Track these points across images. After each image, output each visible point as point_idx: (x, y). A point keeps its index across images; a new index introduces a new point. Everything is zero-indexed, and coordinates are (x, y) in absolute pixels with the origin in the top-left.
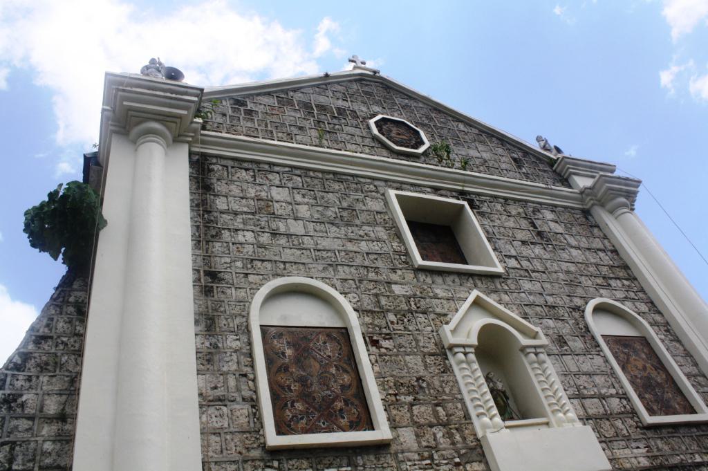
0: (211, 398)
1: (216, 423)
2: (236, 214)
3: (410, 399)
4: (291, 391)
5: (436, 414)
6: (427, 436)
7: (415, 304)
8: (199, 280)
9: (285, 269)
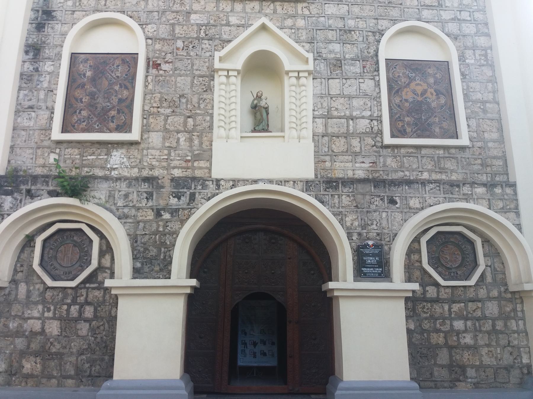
0: (26, 107)
1: (26, 123)
3: (169, 111)
4: (82, 102)
5: (185, 124)
6: (171, 139)
7: (205, 32)
8: (37, 19)
9: (105, 5)
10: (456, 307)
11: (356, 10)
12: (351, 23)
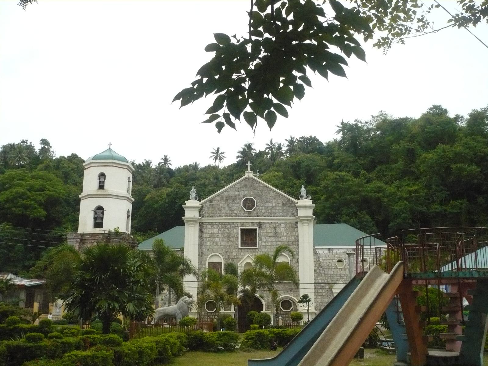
2: (207, 238)
10: (286, 315)
11: (269, 250)
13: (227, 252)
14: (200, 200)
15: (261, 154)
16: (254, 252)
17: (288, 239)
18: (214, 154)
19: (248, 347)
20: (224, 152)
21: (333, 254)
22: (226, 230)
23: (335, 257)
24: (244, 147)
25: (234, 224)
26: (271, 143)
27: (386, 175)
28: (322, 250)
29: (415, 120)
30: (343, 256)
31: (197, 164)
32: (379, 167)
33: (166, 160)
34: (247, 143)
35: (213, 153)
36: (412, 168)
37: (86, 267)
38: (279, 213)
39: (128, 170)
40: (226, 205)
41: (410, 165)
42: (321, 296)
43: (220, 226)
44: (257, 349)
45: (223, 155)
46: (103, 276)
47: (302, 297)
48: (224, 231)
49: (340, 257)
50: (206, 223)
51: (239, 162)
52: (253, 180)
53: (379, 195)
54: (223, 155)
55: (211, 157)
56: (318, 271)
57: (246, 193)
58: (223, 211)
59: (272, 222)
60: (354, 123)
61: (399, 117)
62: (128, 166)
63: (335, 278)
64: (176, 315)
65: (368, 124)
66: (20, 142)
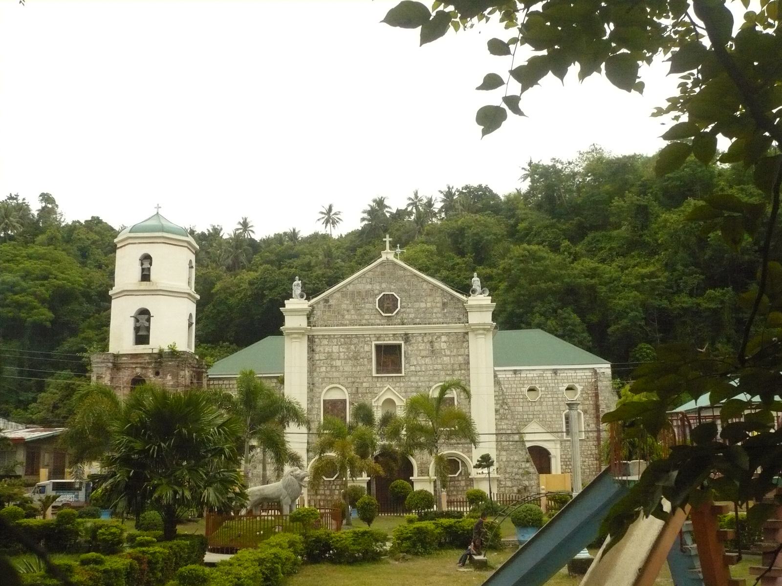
2: (321, 360)
10: (451, 483)
11: (422, 378)
12: (420, 384)
13: (354, 382)
14: (308, 299)
15: (400, 214)
16: (399, 382)
17: (452, 360)
18: (323, 216)
19: (401, 552)
20: (339, 212)
21: (522, 379)
22: (353, 347)
23: (524, 384)
24: (373, 204)
25: (365, 337)
26: (416, 197)
27: (601, 249)
28: (504, 372)
29: (647, 157)
30: (537, 382)
31: (296, 231)
32: (591, 235)
33: (245, 225)
34: (377, 196)
35: (322, 213)
36: (644, 236)
37: (134, 431)
38: (437, 318)
39: (189, 249)
40: (351, 307)
41: (642, 233)
42: (506, 451)
43: (343, 340)
44: (416, 554)
45: (338, 216)
46: (163, 444)
47: (480, 459)
48: (348, 349)
49: (532, 384)
50: (319, 337)
51: (364, 228)
52: (395, 264)
53: (593, 281)
54: (338, 216)
55: (319, 220)
56: (501, 411)
57: (384, 285)
58: (346, 317)
59: (426, 334)
60: (551, 164)
61: (624, 154)
62: (188, 243)
63: (525, 417)
64: (281, 497)
65: (573, 164)
66: (6, 198)
